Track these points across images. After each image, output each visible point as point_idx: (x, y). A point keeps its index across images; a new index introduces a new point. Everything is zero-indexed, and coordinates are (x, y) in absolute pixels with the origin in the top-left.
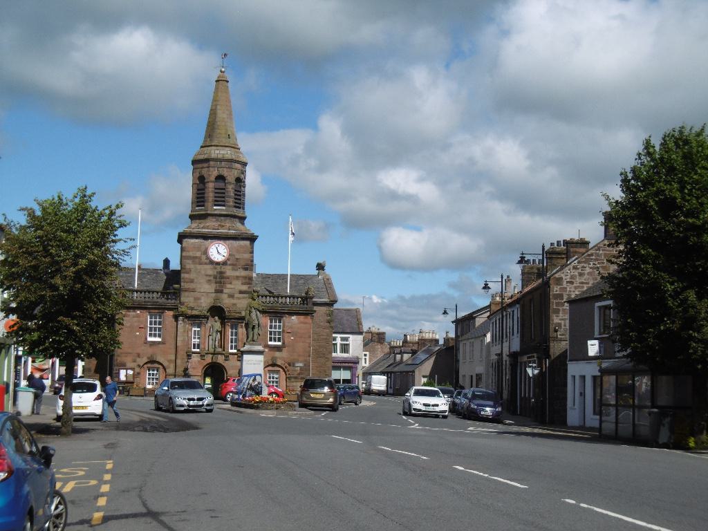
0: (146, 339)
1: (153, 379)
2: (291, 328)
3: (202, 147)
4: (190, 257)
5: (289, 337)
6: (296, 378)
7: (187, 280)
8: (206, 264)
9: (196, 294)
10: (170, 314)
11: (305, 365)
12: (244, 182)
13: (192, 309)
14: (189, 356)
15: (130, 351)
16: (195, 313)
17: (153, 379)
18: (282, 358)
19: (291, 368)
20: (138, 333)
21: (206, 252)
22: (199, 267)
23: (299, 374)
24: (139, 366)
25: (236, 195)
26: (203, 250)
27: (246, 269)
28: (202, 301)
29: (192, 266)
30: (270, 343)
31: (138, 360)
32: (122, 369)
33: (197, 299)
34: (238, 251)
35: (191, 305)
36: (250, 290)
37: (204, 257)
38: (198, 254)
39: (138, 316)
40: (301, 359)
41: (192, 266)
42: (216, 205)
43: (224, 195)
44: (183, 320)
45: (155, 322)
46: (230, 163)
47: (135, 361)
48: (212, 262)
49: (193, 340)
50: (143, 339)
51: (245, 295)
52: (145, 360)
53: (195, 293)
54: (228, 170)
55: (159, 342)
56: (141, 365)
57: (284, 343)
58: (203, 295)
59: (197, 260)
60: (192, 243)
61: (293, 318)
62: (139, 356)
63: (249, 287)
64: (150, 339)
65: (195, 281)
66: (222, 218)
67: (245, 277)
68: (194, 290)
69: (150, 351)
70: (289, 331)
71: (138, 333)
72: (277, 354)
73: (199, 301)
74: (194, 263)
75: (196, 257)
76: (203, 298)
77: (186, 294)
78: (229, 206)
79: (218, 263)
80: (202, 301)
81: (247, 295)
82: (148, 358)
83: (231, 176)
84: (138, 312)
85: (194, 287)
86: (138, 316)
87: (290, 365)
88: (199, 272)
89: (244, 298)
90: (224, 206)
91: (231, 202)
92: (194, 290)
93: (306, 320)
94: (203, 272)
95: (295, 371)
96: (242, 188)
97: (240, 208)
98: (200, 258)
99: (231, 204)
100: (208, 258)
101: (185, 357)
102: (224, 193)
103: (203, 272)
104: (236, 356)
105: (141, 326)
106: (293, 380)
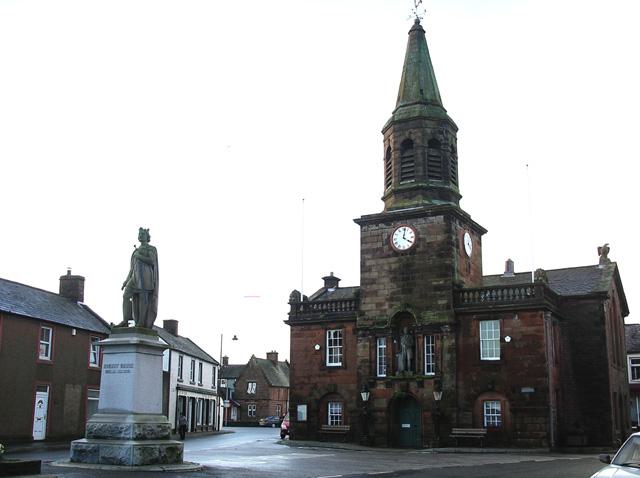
8: (389, 256)
21: (389, 240)
22: (381, 261)
34: (429, 233)
37: (386, 247)
38: (380, 245)
42: (403, 180)
48: (397, 253)
63: (446, 281)
75: (378, 249)
77: (368, 300)
79: (404, 252)
92: (375, 293)
98: (381, 249)
100: (391, 248)
104: (432, 381)
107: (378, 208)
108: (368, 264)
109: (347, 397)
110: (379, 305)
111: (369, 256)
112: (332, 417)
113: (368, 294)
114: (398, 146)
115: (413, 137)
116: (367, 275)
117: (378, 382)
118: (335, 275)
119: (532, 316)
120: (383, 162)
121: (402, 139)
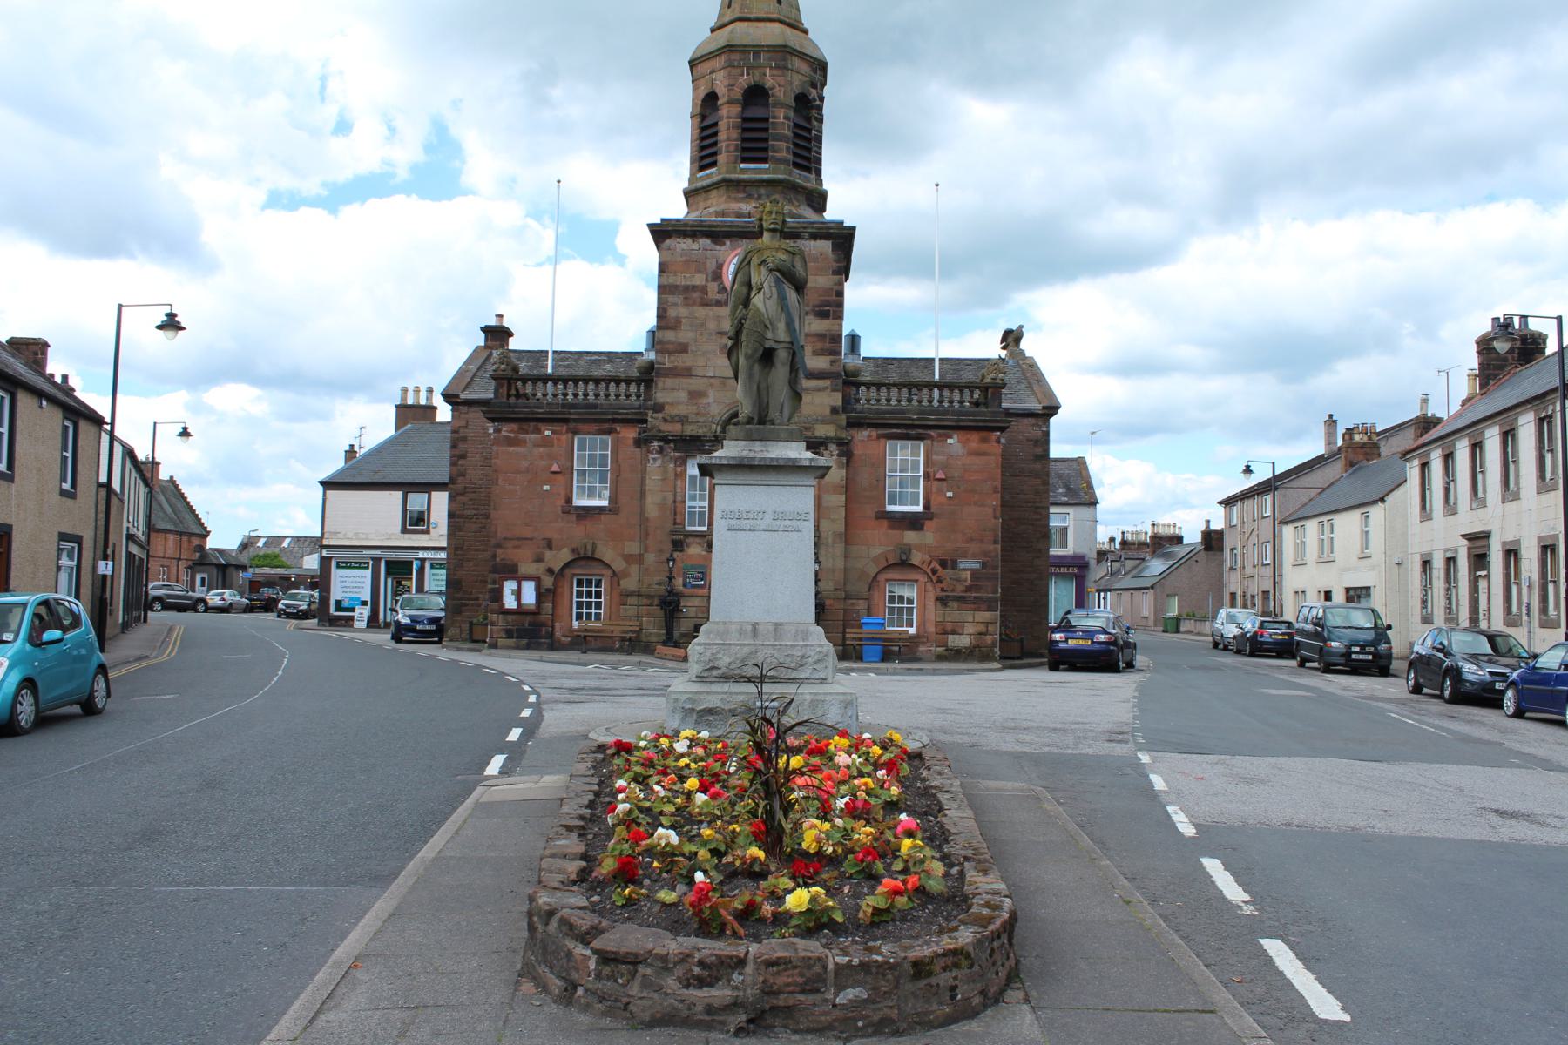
0: (569, 500)
1: (589, 605)
2: (945, 466)
3: (713, 30)
4: (676, 287)
5: (941, 492)
6: (960, 599)
7: (671, 347)
9: (694, 384)
10: (630, 434)
11: (984, 565)
12: (819, 108)
13: (682, 420)
14: (678, 545)
15: (527, 532)
16: (690, 430)
17: (589, 605)
18: (920, 548)
19: (947, 574)
20: (546, 488)
22: (701, 312)
23: (969, 589)
24: (550, 571)
25: (796, 135)
26: (711, 266)
27: (823, 315)
28: (711, 400)
29: (683, 311)
30: (890, 508)
31: (548, 554)
32: (507, 579)
33: (695, 395)
35: (682, 410)
36: (835, 368)
37: (713, 287)
38: (699, 280)
39: (546, 442)
40: (974, 547)
41: (683, 311)
42: (744, 160)
43: (763, 135)
44: (661, 451)
45: (592, 457)
46: (779, 55)
47: (539, 559)
49: (688, 503)
50: (561, 502)
51: (821, 383)
52: (565, 555)
53: (692, 380)
54: (775, 72)
55: (600, 509)
56: (557, 569)
57: (927, 506)
58: (712, 385)
59: (696, 295)
60: (684, 253)
61: (949, 441)
62: (549, 545)
63: (832, 362)
64: (580, 502)
65: (692, 348)
66: (763, 191)
67: (821, 336)
68: (687, 373)
69: (578, 533)
70: (940, 475)
71: (546, 488)
72: (910, 537)
73: (704, 401)
74: (687, 302)
75: (694, 288)
76: (711, 393)
77: (669, 382)
78: (779, 161)
80: (711, 400)
81: (827, 383)
82: (574, 551)
83: (782, 86)
84: (547, 433)
85: (689, 364)
86: (546, 442)
87: (943, 564)
88: (703, 325)
89: (819, 390)
90: (765, 160)
91: (783, 150)
92: (687, 373)
93: (985, 447)
94: (712, 326)
95: (958, 580)
96: (815, 123)
97: (808, 170)
98: (704, 290)
99: (783, 154)
101: (669, 547)
102: (766, 130)
103: (712, 326)
105: (555, 468)
106: (955, 605)
107: (677, 209)
108: (672, 313)
109: (619, 565)
110: (695, 395)
111: (678, 299)
112: (580, 605)
113: (673, 372)
114: (738, 94)
115: (769, 82)
116: (669, 335)
117: (690, 540)
118: (506, 323)
119: (984, 440)
120: (689, 122)
121: (744, 81)
